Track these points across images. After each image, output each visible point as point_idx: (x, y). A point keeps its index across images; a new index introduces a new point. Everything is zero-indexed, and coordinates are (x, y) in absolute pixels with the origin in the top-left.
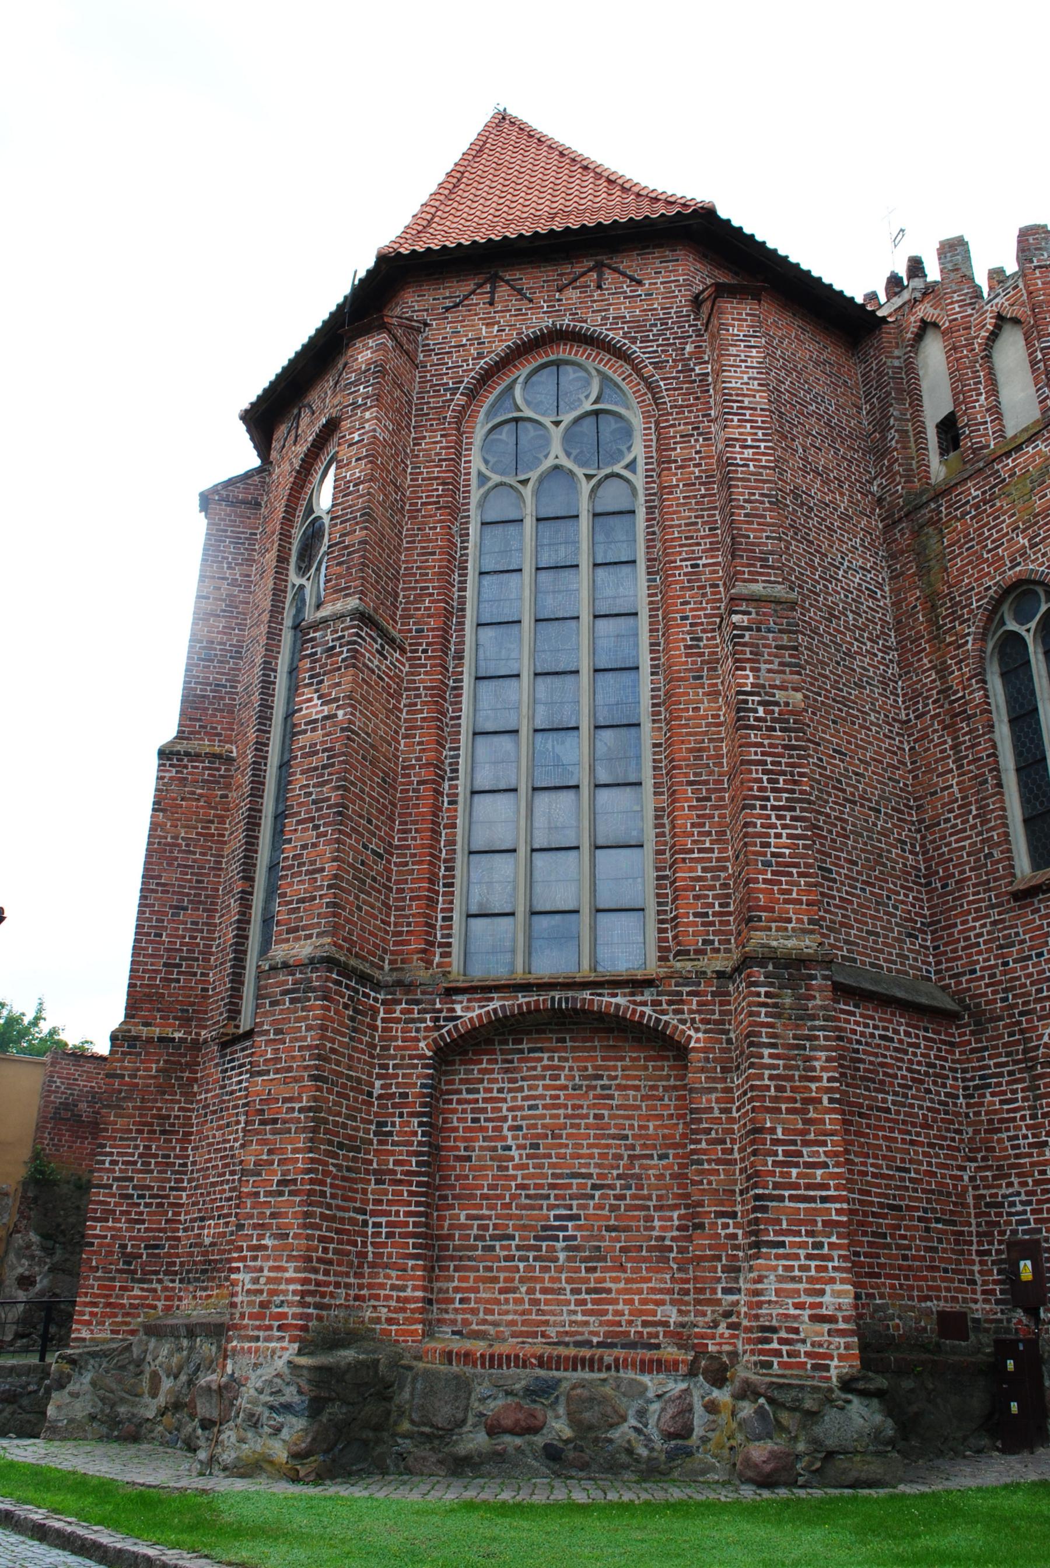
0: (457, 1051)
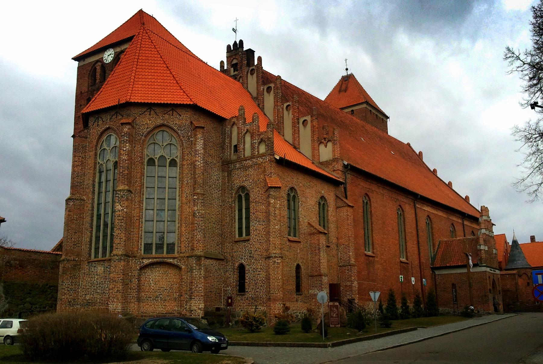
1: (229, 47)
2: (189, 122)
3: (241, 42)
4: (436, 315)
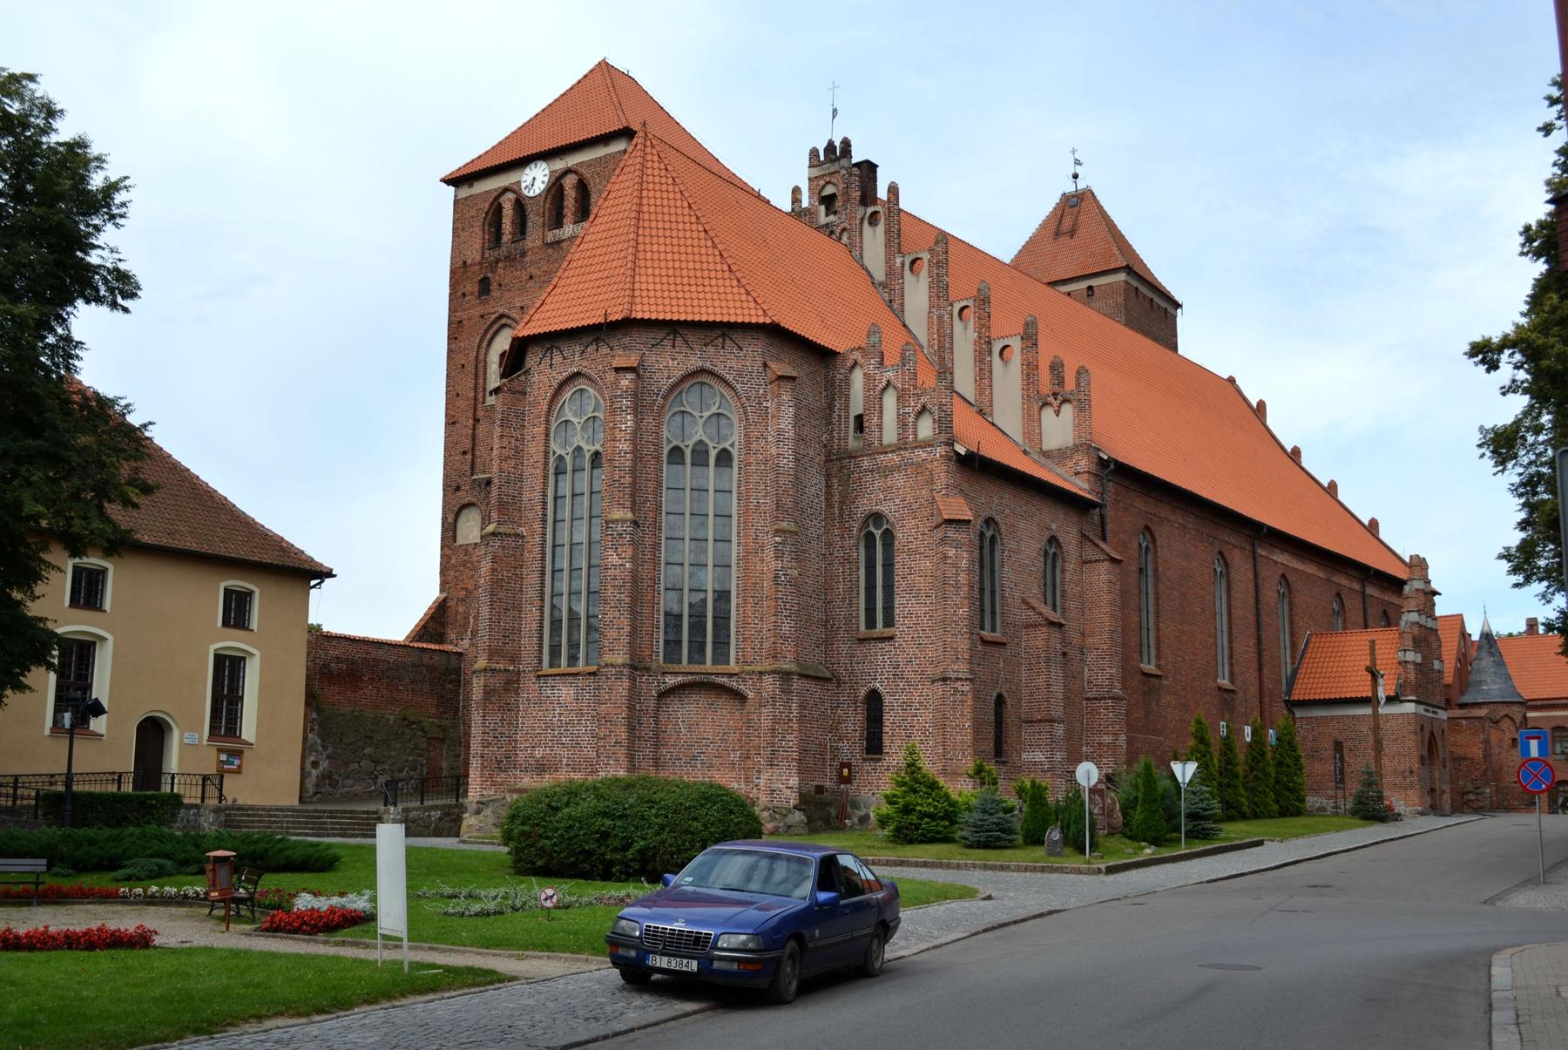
0: (665, 694)
1: (814, 153)
2: (759, 363)
3: (846, 144)
4: (1298, 813)
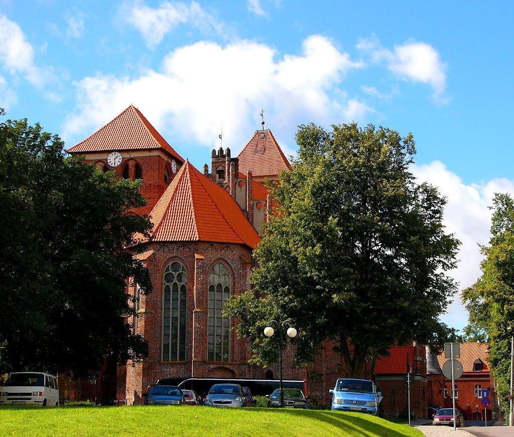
1: (214, 151)
3: (229, 150)
